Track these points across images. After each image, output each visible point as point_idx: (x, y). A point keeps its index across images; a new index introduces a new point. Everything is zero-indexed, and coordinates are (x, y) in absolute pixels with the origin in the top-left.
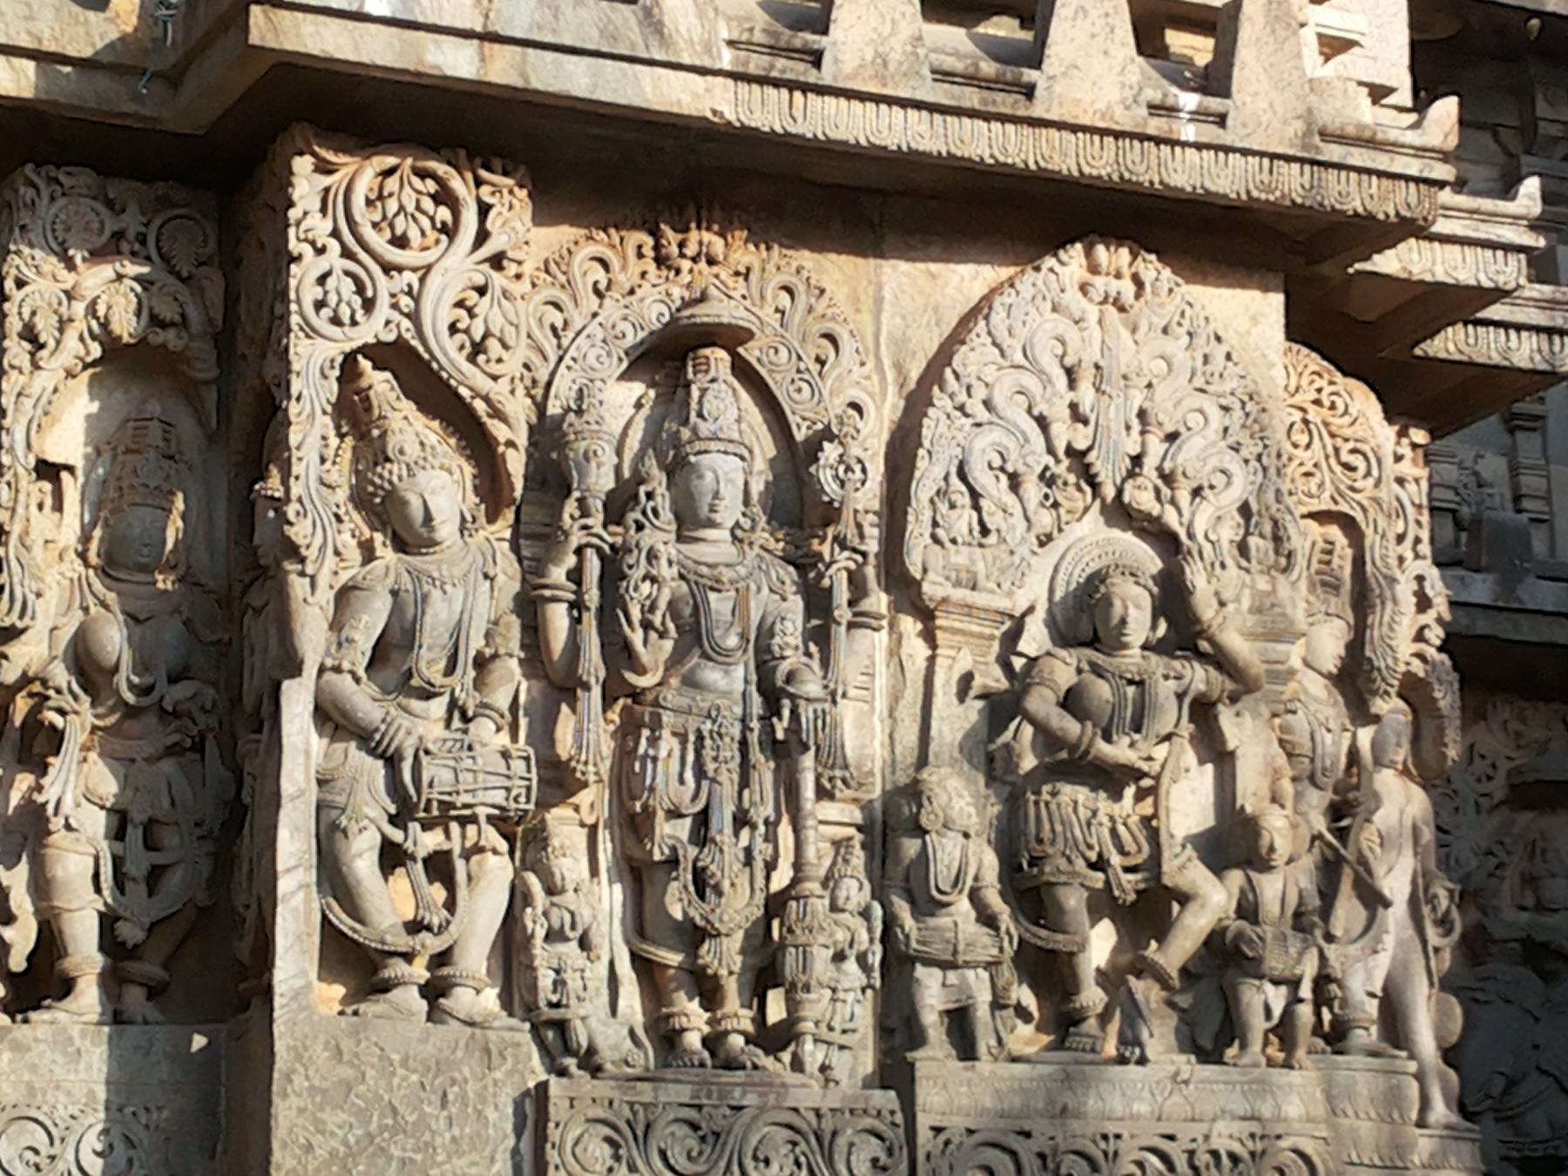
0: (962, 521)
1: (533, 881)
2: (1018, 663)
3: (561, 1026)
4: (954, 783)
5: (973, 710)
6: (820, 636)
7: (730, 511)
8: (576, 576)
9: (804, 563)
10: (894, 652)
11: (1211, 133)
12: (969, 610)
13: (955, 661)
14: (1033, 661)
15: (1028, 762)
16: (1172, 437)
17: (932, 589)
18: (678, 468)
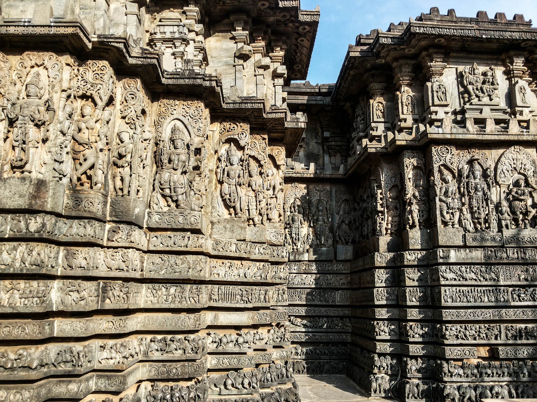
0: (503, 175)
3: (466, 228)
4: (504, 202)
6: (489, 188)
7: (479, 177)
9: (486, 181)
10: (496, 189)
11: (528, 133)
13: (503, 190)
14: (511, 189)
15: (511, 199)
17: (500, 183)
18: (473, 173)
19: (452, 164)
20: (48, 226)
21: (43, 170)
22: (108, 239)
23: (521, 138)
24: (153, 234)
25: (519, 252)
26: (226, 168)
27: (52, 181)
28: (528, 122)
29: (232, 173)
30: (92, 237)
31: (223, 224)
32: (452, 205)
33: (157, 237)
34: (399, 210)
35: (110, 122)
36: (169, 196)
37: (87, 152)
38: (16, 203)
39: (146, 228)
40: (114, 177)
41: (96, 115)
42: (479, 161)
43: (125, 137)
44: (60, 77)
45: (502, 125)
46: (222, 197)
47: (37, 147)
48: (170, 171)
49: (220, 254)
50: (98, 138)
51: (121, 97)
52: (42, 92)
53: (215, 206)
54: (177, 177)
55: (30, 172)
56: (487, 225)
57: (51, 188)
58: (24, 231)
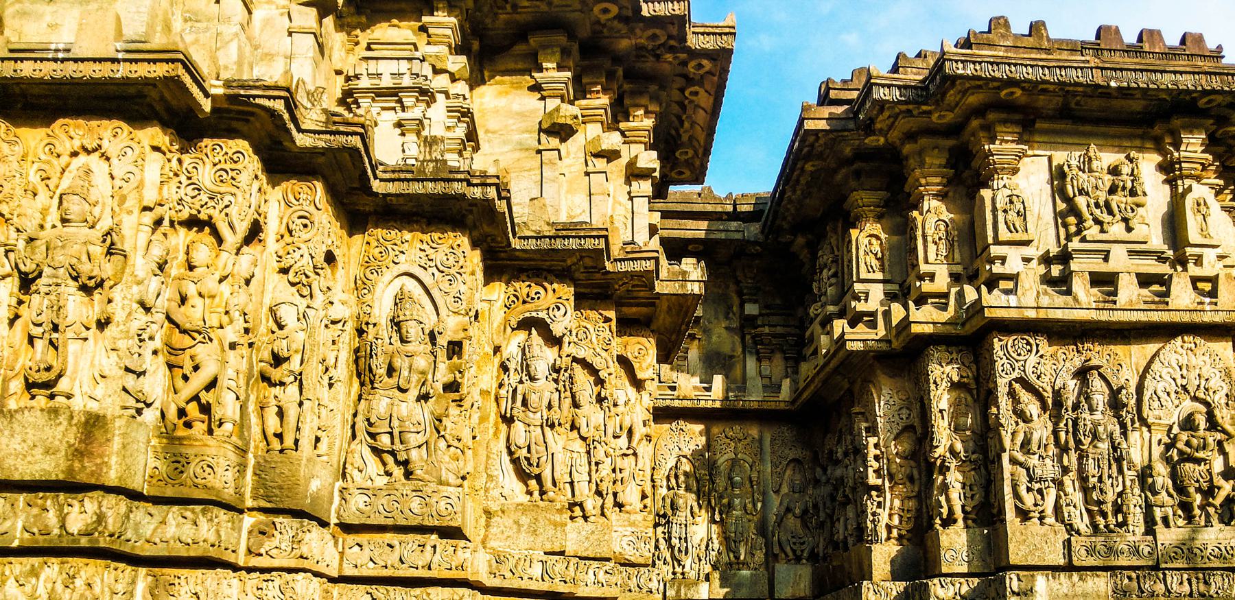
0: (1156, 404)
1: (1061, 493)
2: (1172, 436)
3: (1071, 525)
4: (1160, 465)
5: (1162, 447)
6: (1124, 434)
7: (1101, 408)
8: (1066, 425)
9: (1118, 416)
10: (1141, 435)
12: (1159, 425)
14: (1176, 435)
15: (1176, 458)
16: (1207, 380)
17: (1150, 421)
18: (1088, 399)
19: (1039, 377)
20: (110, 521)
21: (99, 392)
22: (249, 551)
23: (1197, 318)
24: (352, 539)
25: (1194, 581)
26: (520, 387)
27: (120, 417)
28: (1214, 280)
29: (533, 399)
30: (213, 546)
31: (514, 516)
32: (1038, 471)
33: (360, 546)
34: (917, 483)
35: (253, 281)
36: (388, 452)
37: (200, 347)
38: (37, 467)
39: (336, 525)
40: (262, 408)
41: (221, 265)
42: (1101, 370)
43: (288, 315)
44: (138, 177)
45: (1156, 288)
46: (511, 453)
47: (86, 339)
48: (390, 393)
49: (506, 584)
50: (225, 319)
51: (277, 222)
52: (97, 211)
53: (496, 473)
54: (408, 409)
55: (69, 397)
56: (1120, 518)
57: (117, 432)
58: (56, 531)
